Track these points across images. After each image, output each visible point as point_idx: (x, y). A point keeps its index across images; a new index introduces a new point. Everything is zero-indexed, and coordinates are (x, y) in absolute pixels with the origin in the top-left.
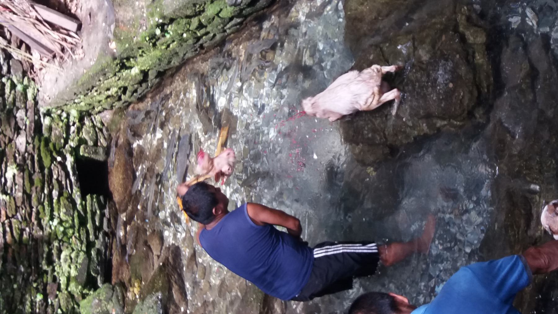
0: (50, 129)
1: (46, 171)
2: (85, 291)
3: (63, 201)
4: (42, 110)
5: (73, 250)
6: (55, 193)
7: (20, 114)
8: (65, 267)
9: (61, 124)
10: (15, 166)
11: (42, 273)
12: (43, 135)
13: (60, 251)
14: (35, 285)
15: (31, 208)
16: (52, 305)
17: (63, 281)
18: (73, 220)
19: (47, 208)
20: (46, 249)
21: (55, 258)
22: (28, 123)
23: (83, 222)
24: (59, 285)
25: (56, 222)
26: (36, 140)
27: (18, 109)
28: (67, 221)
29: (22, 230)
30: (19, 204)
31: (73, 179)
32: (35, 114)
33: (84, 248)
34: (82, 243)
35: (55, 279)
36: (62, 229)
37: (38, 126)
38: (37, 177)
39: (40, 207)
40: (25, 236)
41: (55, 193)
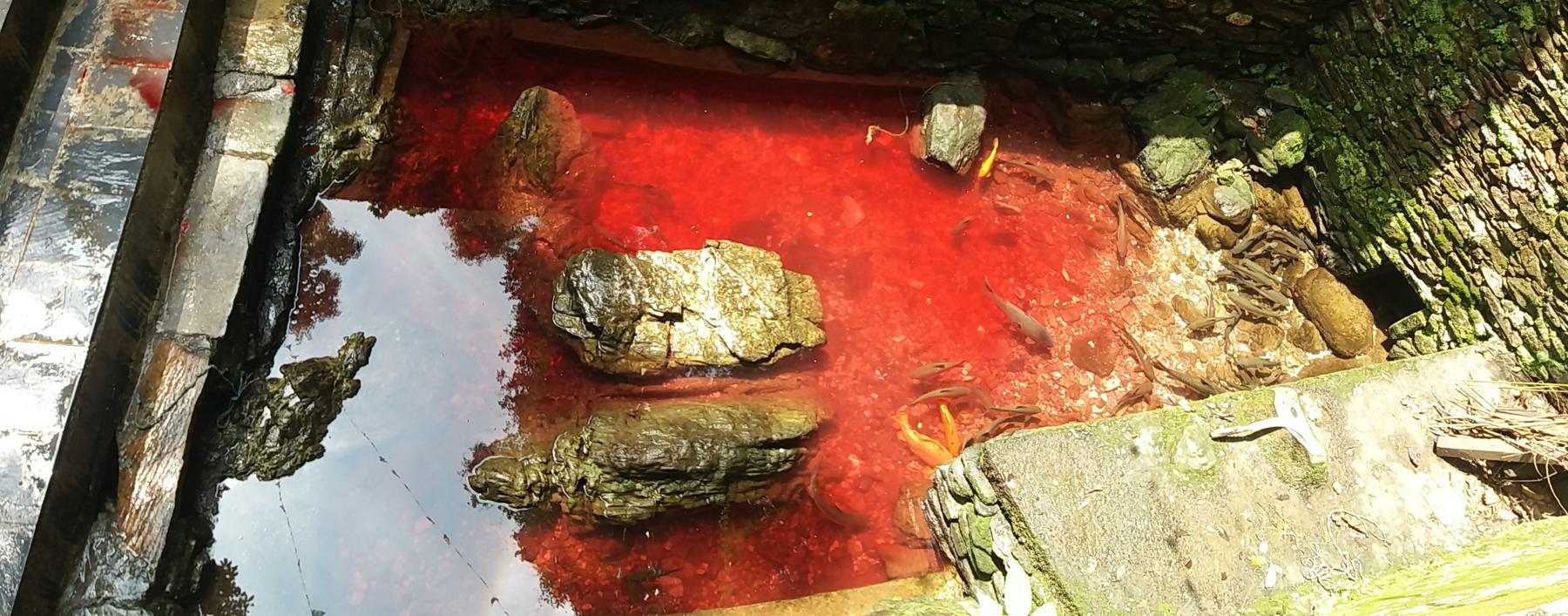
0: (1471, 321)
1: (1444, 262)
3: (1400, 235)
6: (1416, 239)
7: (1518, 317)
9: (1464, 336)
10: (1478, 240)
13: (1369, 173)
15: (1431, 204)
20: (1383, 164)
26: (1477, 293)
27: (1526, 323)
30: (1445, 197)
31: (1409, 272)
35: (1355, 138)
38: (1448, 245)
41: (1416, 239)
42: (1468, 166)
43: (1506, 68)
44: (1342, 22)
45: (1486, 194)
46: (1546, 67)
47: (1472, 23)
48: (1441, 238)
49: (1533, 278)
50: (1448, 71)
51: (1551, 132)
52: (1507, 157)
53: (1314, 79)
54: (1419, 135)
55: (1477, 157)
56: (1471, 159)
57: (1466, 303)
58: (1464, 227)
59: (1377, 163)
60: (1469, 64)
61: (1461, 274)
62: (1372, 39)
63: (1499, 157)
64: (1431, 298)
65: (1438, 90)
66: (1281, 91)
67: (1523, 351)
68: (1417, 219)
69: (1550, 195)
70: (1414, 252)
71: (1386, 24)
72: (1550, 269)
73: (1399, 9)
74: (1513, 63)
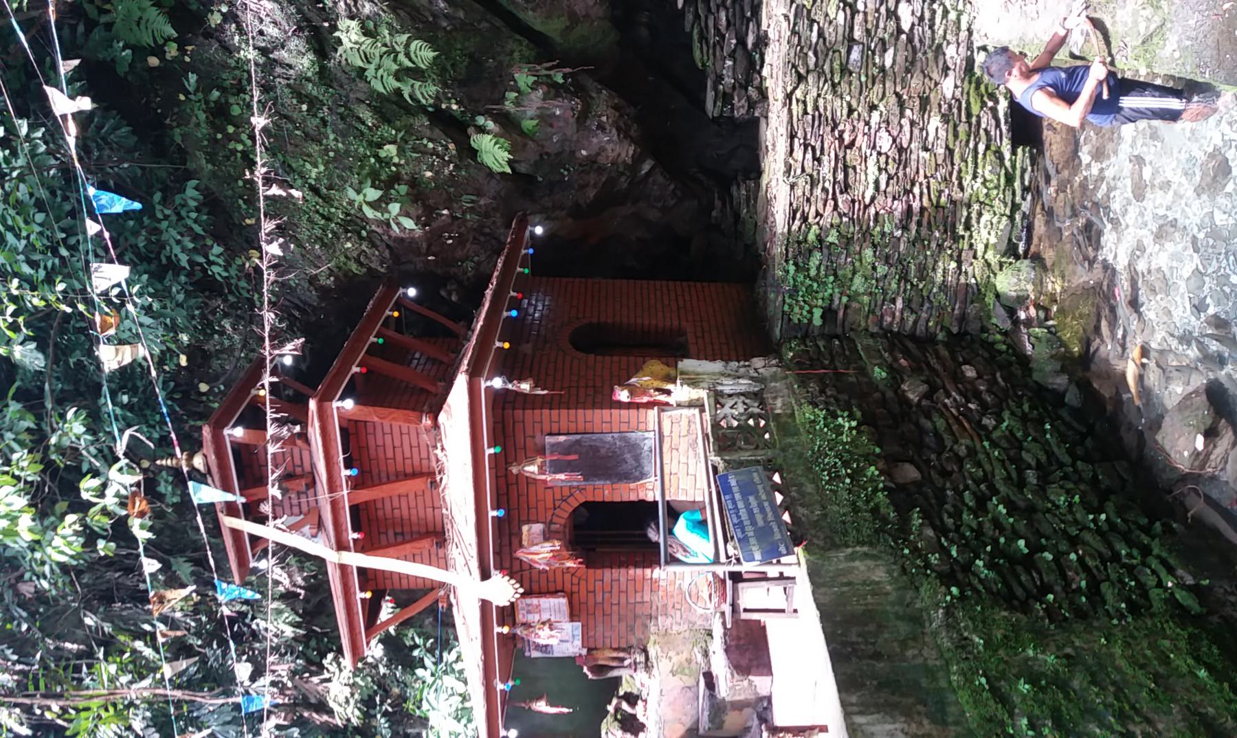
1: (974, 120)
2: (1004, 259)
3: (990, 157)
4: (976, 45)
5: (995, 214)
6: (981, 147)
7: (950, 51)
8: (984, 233)
10: (939, 118)
11: (956, 238)
12: (974, 74)
13: (980, 214)
14: (949, 252)
15: (953, 164)
16: (966, 273)
17: (980, 248)
18: (999, 180)
19: (970, 164)
20: (965, 213)
21: (974, 222)
22: (958, 62)
23: (1010, 179)
25: (980, 180)
26: (966, 83)
27: (949, 43)
28: (991, 181)
29: (940, 192)
30: (940, 162)
31: (1004, 128)
33: (1008, 212)
34: (1006, 205)
36: (985, 191)
37: (970, 62)
38: (962, 128)
40: (943, 199)
41: (981, 147)
43: (845, 214)
44: (921, 328)
45: (912, 146)
46: (824, 196)
47: (843, 256)
48: (962, 136)
49: (923, 72)
50: (877, 239)
51: (848, 157)
53: (972, 310)
54: (926, 214)
55: (901, 174)
56: (905, 174)
57: (979, 82)
60: (864, 235)
61: (968, 103)
62: (910, 301)
63: (887, 163)
65: (892, 233)
66: (999, 319)
67: (964, 26)
69: (875, 116)
71: (893, 301)
72: (908, 71)
73: (879, 302)
74: (839, 214)
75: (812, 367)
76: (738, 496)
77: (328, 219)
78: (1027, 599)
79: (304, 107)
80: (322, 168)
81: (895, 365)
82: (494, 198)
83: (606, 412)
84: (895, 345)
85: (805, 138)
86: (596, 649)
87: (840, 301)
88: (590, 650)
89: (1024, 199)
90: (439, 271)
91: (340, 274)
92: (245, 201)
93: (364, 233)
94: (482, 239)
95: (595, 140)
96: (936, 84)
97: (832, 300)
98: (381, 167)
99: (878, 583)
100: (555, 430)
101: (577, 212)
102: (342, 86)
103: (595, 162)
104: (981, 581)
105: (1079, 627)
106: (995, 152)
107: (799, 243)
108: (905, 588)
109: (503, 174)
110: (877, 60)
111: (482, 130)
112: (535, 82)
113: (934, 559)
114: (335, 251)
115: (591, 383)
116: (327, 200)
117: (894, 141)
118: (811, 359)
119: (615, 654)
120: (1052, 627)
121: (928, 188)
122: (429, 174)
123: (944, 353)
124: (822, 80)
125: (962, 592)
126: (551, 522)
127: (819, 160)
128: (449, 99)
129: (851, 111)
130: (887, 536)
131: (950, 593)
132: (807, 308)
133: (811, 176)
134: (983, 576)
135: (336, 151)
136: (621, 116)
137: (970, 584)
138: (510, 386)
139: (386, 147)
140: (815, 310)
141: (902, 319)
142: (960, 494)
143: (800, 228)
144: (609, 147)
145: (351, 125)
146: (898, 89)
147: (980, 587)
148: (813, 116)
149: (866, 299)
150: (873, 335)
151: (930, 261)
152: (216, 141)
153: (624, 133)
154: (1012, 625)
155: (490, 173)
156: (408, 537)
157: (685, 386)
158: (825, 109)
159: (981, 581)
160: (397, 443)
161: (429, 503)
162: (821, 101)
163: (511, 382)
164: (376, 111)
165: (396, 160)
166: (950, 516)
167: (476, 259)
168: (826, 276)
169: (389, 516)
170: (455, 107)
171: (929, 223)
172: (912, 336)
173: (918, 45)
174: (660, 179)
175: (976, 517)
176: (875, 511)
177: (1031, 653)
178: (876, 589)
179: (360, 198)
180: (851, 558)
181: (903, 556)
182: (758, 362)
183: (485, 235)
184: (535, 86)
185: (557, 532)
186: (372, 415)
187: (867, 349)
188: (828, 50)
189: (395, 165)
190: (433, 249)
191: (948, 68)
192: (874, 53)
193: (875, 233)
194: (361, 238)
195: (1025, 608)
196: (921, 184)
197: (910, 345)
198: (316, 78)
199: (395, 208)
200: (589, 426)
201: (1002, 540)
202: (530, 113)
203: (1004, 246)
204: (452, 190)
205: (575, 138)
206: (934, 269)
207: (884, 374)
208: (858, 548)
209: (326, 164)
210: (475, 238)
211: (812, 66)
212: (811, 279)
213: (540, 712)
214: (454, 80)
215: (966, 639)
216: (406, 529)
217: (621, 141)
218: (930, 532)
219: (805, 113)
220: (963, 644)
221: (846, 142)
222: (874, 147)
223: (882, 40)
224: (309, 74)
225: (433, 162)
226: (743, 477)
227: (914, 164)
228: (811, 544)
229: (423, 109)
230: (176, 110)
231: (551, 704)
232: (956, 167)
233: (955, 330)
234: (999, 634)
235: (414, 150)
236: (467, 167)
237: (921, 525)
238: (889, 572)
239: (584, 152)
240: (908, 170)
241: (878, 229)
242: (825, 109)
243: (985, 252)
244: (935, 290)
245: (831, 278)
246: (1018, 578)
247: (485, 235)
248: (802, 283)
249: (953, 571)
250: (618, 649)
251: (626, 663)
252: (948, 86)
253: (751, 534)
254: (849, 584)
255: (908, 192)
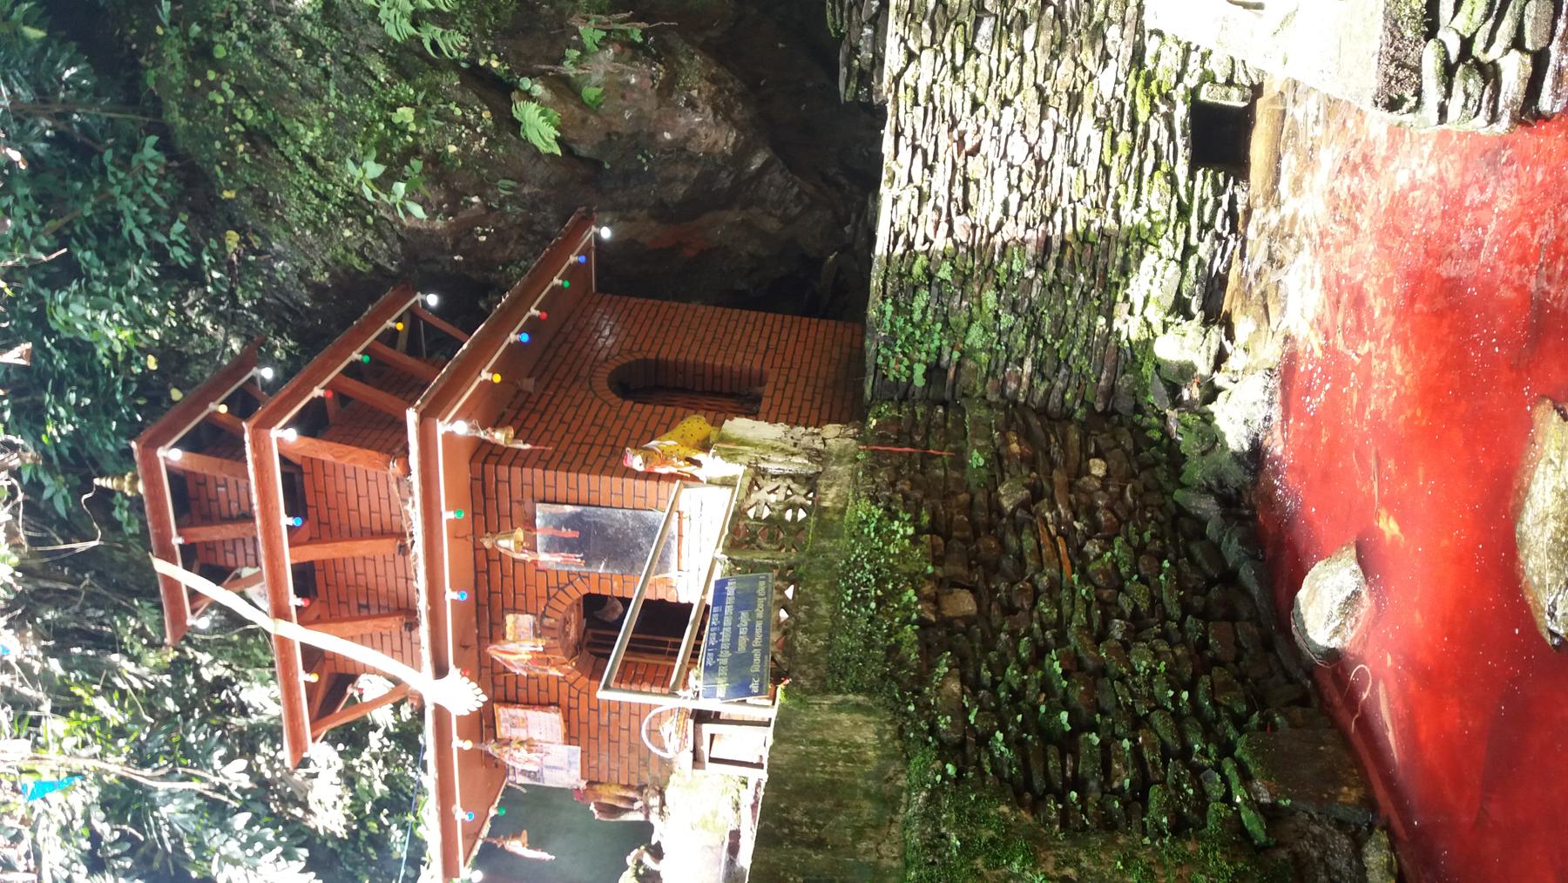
0: (1158, 57)
2: (1170, 319)
4: (1148, 26)
7: (1113, 33)
9: (1175, 47)
13: (1141, 256)
14: (1097, 303)
15: (1108, 187)
18: (1168, 212)
19: (1132, 191)
20: (1120, 253)
23: (1184, 212)
24: (1132, 306)
25: (1143, 210)
26: (1132, 77)
27: (1111, 22)
28: (1158, 212)
29: (1089, 223)
30: (1090, 182)
31: (1180, 142)
32: (1136, 32)
34: (1176, 247)
36: (1148, 225)
38: (1124, 139)
39: (1122, 189)
42: (1052, 191)
44: (1055, 399)
47: (957, 298)
48: (1123, 150)
49: (1074, 59)
50: (1003, 280)
52: (1015, 173)
53: (1124, 382)
54: (1069, 250)
56: (1043, 195)
58: (1095, 145)
59: (1125, 258)
64: (1179, 103)
66: (1156, 396)
68: (1131, 182)
70: (1158, 157)
71: (1021, 362)
73: (1001, 363)
74: (955, 242)
75: (897, 442)
76: (729, 610)
77: (324, 197)
78: (1047, 792)
79: (299, 53)
80: (318, 132)
81: (1003, 451)
82: (542, 186)
83: (617, 481)
84: (1013, 419)
85: (914, 138)
86: (598, 783)
87: (950, 357)
88: (590, 783)
89: (1201, 239)
90: (474, 276)
91: (338, 269)
92: (223, 167)
93: (370, 219)
94: (531, 238)
95: (682, 121)
96: (1091, 77)
97: (940, 355)
98: (394, 135)
99: (859, 746)
100: (550, 493)
101: (662, 212)
102: (349, 29)
103: (684, 149)
104: (992, 756)
105: (1097, 841)
106: (1166, 175)
107: (901, 276)
108: (892, 757)
109: (552, 155)
110: (1014, 40)
111: (528, 96)
112: (603, 39)
113: (943, 723)
114: (331, 240)
115: (611, 441)
116: (324, 174)
117: (1031, 149)
118: (899, 432)
119: (623, 793)
120: (1061, 836)
121: (1074, 216)
122: (452, 149)
123: (1074, 436)
124: (940, 60)
125: (959, 772)
126: (544, 615)
127: (931, 169)
128: (489, 55)
129: (976, 105)
130: (894, 684)
131: (944, 772)
132: (906, 362)
133: (920, 189)
134: (997, 754)
135: (338, 112)
136: (720, 91)
137: (979, 764)
138: (482, 434)
139: (400, 110)
140: (916, 366)
141: (1031, 387)
142: (1014, 636)
143: (902, 257)
144: (702, 131)
145: (358, 80)
146: (1040, 80)
147: (988, 769)
148: (926, 109)
149: (984, 356)
150: (989, 406)
151: (1071, 312)
152: (193, 87)
153: (723, 112)
154: (1010, 826)
155: (536, 153)
156: (374, 611)
157: (718, 458)
158: (942, 99)
159: (993, 760)
160: (363, 492)
161: (401, 573)
162: (936, 88)
163: (484, 428)
164: (391, 62)
165: (413, 128)
166: (990, 667)
167: (523, 263)
168: (934, 323)
169: (351, 582)
170: (495, 64)
171: (1072, 262)
172: (1042, 412)
173: (1070, 22)
174: (778, 178)
175: (1024, 671)
176: (892, 650)
177: (1016, 867)
178: (853, 754)
179: (359, 173)
180: (837, 708)
181: (906, 714)
182: (831, 430)
183: (534, 233)
184: (603, 45)
185: (551, 628)
186: (323, 451)
187: (976, 422)
188: (949, 21)
189: (412, 134)
190: (462, 246)
191: (1108, 56)
192: (1010, 29)
193: (1000, 271)
194: (365, 225)
195: (1036, 806)
196: (1064, 211)
197: (1035, 422)
198: (318, 16)
199: (400, 188)
200: (594, 496)
201: (1043, 709)
202: (596, 78)
203: (1169, 301)
204: (485, 171)
205: (655, 116)
206: (1075, 325)
207: (982, 462)
208: (851, 697)
209: (325, 127)
210: (521, 237)
211: (927, 43)
212: (913, 325)
213: (513, 855)
214: (496, 28)
215: (943, 836)
216: (373, 602)
217: (718, 125)
218: (955, 686)
219: (916, 103)
220: (936, 843)
221: (968, 147)
222: (1005, 156)
223: (1022, 12)
224: (309, 11)
225: (462, 134)
226: (746, 585)
227: (1056, 183)
228: (795, 683)
229: (455, 64)
230: (153, 47)
231: (533, 844)
232: (1112, 192)
233: (1099, 407)
234: (987, 834)
235: (438, 116)
236: (507, 143)
237: (946, 675)
238: (880, 734)
239: (667, 136)
240: (1048, 189)
241: (1004, 265)
242: (942, 99)
243: (1145, 306)
244: (1075, 352)
245: (939, 326)
246: (1046, 759)
247: (534, 233)
248: (903, 330)
249: (964, 742)
250: (628, 787)
251: (637, 805)
252: (1106, 82)
253: (725, 661)
254: (823, 742)
255: (1046, 219)
